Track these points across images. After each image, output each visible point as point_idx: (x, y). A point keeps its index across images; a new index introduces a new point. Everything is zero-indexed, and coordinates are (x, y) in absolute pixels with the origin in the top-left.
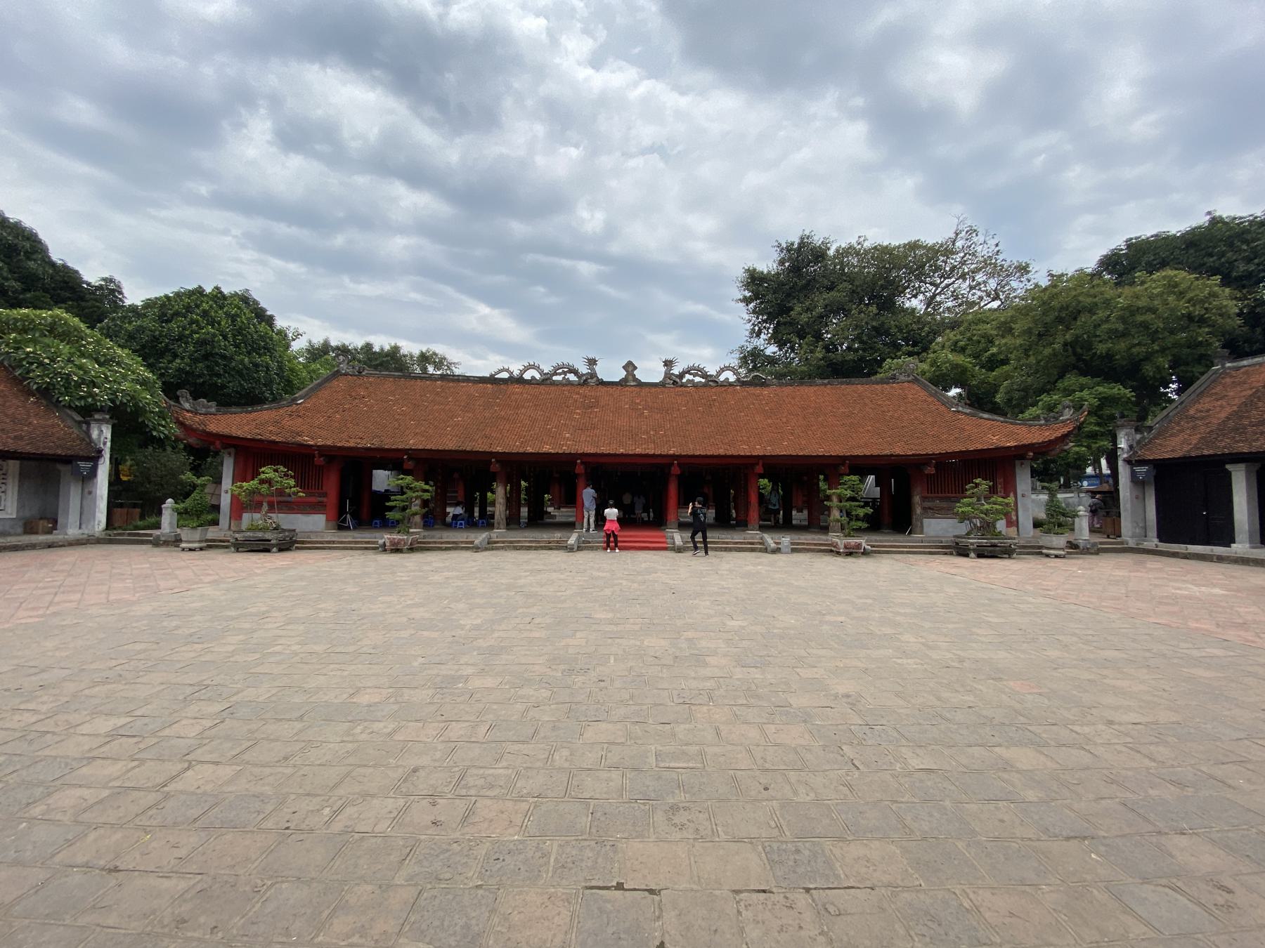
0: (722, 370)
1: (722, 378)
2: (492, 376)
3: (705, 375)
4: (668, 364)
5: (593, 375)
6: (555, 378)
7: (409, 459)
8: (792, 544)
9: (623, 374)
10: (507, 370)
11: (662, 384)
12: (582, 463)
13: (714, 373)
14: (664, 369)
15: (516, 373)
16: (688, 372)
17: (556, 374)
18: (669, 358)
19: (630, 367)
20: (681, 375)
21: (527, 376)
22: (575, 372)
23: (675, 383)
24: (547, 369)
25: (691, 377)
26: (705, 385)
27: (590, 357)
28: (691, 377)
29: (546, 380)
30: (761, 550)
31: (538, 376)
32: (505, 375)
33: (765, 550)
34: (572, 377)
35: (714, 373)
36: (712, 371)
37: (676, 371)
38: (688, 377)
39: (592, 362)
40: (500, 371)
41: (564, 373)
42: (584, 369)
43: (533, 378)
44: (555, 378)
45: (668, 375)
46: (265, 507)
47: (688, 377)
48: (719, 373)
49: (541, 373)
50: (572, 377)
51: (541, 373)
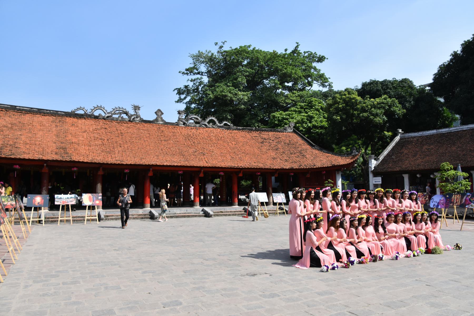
6: (114, 116)
7: (47, 166)
9: (155, 117)
15: (89, 112)
17: (115, 114)
19: (159, 113)
21: (96, 113)
22: (126, 113)
27: (136, 104)
31: (103, 114)
32: (81, 112)
39: (136, 108)
41: (120, 113)
42: (132, 112)
44: (114, 116)
50: (124, 116)
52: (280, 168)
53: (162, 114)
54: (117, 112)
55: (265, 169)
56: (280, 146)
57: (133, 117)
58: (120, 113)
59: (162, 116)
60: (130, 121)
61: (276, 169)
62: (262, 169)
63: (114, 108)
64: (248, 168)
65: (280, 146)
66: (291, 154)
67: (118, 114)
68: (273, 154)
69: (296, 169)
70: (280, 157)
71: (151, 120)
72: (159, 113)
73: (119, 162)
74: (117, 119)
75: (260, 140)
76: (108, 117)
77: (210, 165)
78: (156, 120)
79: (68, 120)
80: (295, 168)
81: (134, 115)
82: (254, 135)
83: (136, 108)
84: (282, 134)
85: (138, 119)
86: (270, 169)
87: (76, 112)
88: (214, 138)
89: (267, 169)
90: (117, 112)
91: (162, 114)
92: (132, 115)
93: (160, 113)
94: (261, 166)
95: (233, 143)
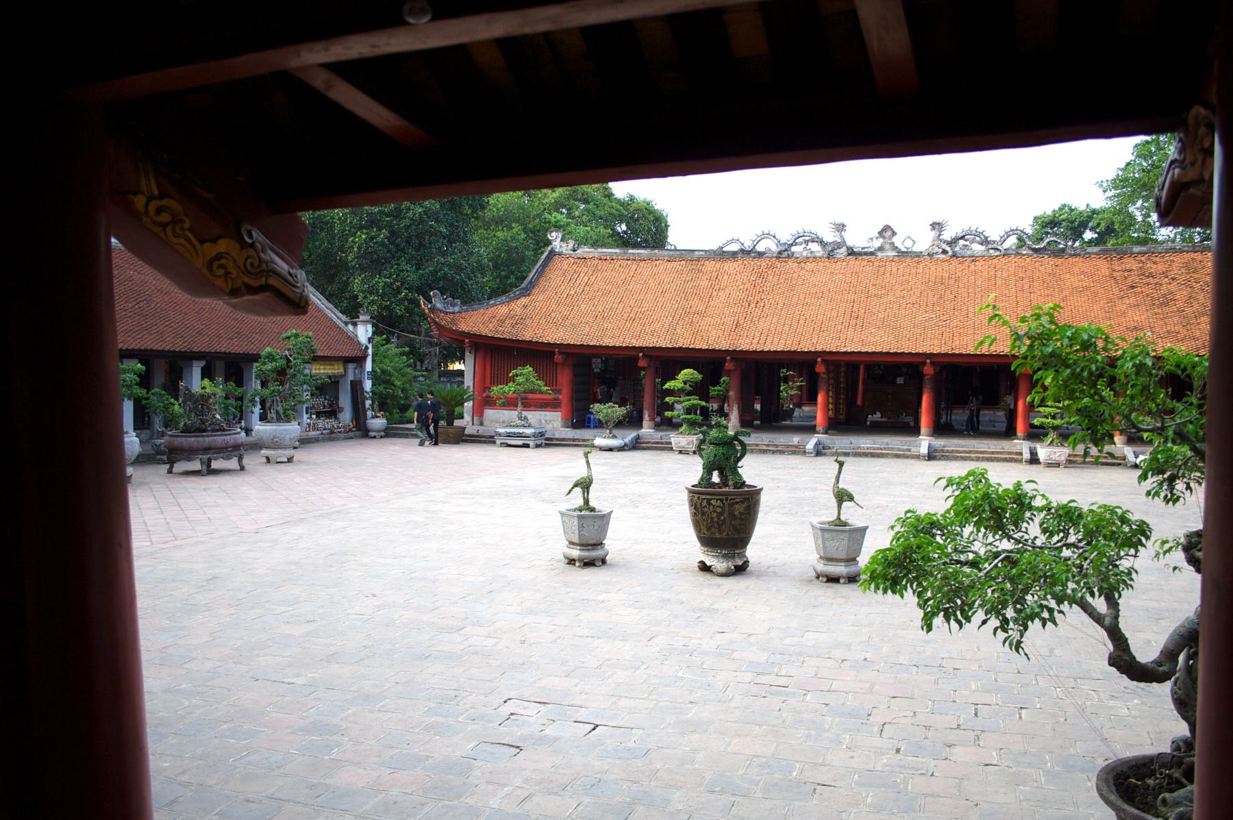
3: (985, 241)
4: (937, 226)
6: (794, 249)
15: (748, 245)
16: (962, 238)
19: (886, 231)
20: (953, 243)
21: (760, 248)
23: (945, 252)
24: (785, 237)
29: (784, 253)
30: (1016, 461)
31: (774, 248)
32: (734, 247)
36: (994, 236)
37: (948, 235)
39: (840, 228)
40: (727, 244)
41: (807, 242)
42: (830, 237)
47: (962, 242)
50: (815, 247)
53: (894, 233)
58: (807, 242)
59: (895, 239)
76: (780, 253)
77: (944, 350)
79: (709, 266)
83: (840, 228)
85: (843, 250)
91: (894, 233)
93: (888, 234)
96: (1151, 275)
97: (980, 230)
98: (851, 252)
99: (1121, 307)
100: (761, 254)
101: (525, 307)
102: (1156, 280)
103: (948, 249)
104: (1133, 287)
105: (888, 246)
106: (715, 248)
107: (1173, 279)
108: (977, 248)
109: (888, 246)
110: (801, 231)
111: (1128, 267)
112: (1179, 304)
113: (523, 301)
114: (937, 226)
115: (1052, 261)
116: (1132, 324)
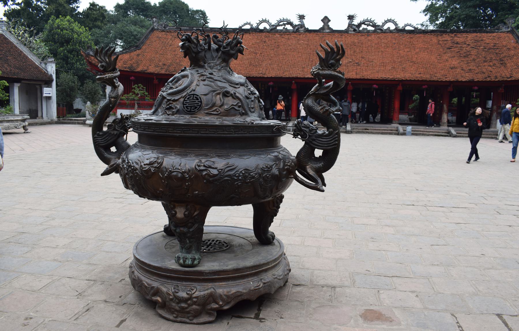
0: (386, 22)
1: (385, 27)
2: (240, 27)
3: (374, 25)
4: (351, 18)
5: (302, 25)
6: (278, 28)
8: (412, 131)
9: (321, 25)
10: (249, 24)
11: (346, 31)
12: (295, 82)
13: (381, 24)
14: (347, 21)
16: (364, 23)
17: (279, 25)
18: (352, 14)
19: (326, 20)
20: (359, 25)
21: (261, 27)
22: (291, 24)
23: (355, 30)
24: (274, 22)
25: (365, 27)
26: (374, 31)
27: (301, 14)
28: (365, 27)
29: (273, 30)
30: (395, 134)
31: (268, 27)
32: (248, 27)
33: (398, 134)
34: (289, 27)
35: (381, 24)
36: (379, 23)
37: (356, 22)
38: (363, 26)
39: (302, 17)
40: (245, 24)
41: (284, 25)
42: (296, 22)
43: (265, 28)
44: (278, 28)
45: (350, 25)
46: (136, 106)
47: (363, 26)
48: (384, 24)
49: (270, 25)
50: (289, 27)
51: (270, 25)
52: (452, 80)
53: (330, 21)
54: (282, 23)
55: (430, 81)
56: (474, 52)
57: (297, 28)
58: (284, 25)
59: (329, 24)
60: (293, 32)
61: (446, 81)
62: (426, 81)
63: (278, 19)
64: (407, 80)
65: (474, 52)
66: (485, 61)
67: (281, 25)
68: (455, 62)
69: (478, 81)
70: (464, 66)
71: (317, 28)
72: (326, 20)
73: (261, 75)
74: (281, 30)
75: (449, 44)
76: (271, 30)
77: (358, 77)
78: (322, 29)
80: (476, 80)
81: (298, 25)
82: (443, 39)
83: (302, 17)
84: (490, 35)
86: (438, 81)
87: (243, 28)
88: (383, 45)
89: (434, 81)
90: (282, 23)
91: (330, 21)
92: (296, 26)
93: (326, 21)
94: (427, 77)
95: (406, 50)
96: (457, 43)
97: (372, 20)
98: (308, 31)
99: (445, 57)
100: (261, 31)
101: (138, 55)
102: (460, 46)
103: (357, 29)
104: (450, 49)
105: (326, 27)
106: (238, 27)
107: (469, 45)
108: (370, 28)
109: (326, 27)
110: (282, 18)
111: (446, 39)
112: (473, 57)
113: (138, 52)
114: (351, 18)
115: (409, 35)
116: (452, 66)
